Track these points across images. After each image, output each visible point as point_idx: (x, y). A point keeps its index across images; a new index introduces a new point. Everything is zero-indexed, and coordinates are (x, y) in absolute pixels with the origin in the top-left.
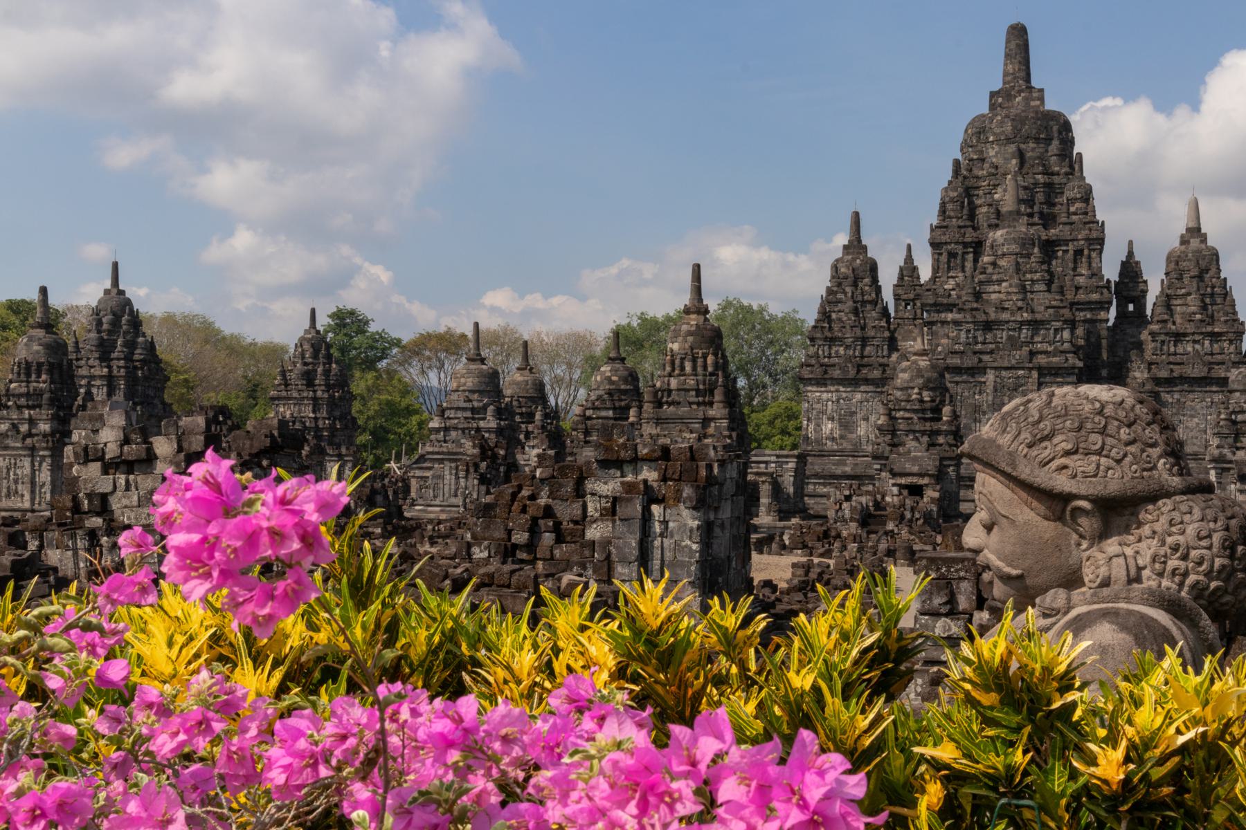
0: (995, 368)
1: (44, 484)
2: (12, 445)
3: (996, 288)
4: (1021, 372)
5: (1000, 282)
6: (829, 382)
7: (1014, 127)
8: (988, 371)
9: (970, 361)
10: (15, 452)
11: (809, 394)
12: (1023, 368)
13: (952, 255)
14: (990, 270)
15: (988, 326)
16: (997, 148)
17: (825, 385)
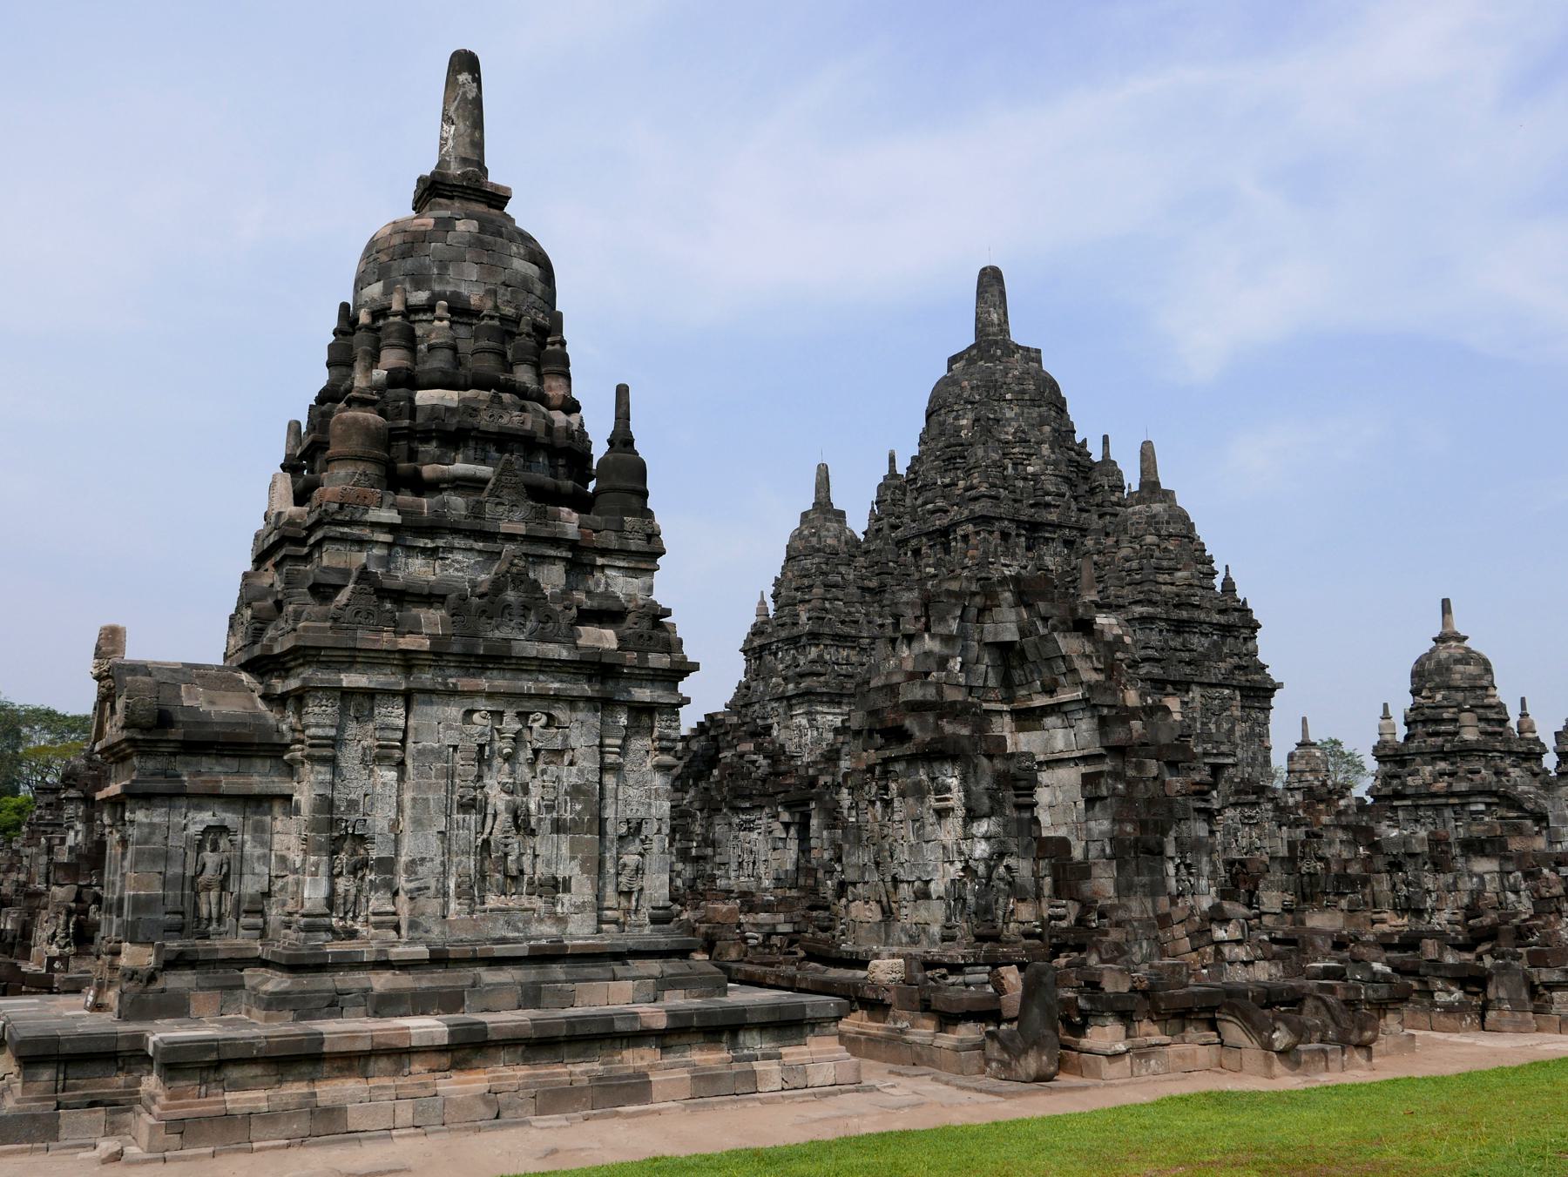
0: (1201, 684)
1: (636, 828)
2: (533, 649)
3: (1167, 578)
4: (1226, 692)
5: (1172, 571)
6: (845, 700)
7: (1038, 388)
8: (1194, 687)
9: (1176, 673)
10: (527, 685)
11: (819, 717)
12: (1227, 687)
13: (1005, 536)
14: (1157, 553)
15: (1180, 627)
16: (1016, 409)
17: (839, 704)
